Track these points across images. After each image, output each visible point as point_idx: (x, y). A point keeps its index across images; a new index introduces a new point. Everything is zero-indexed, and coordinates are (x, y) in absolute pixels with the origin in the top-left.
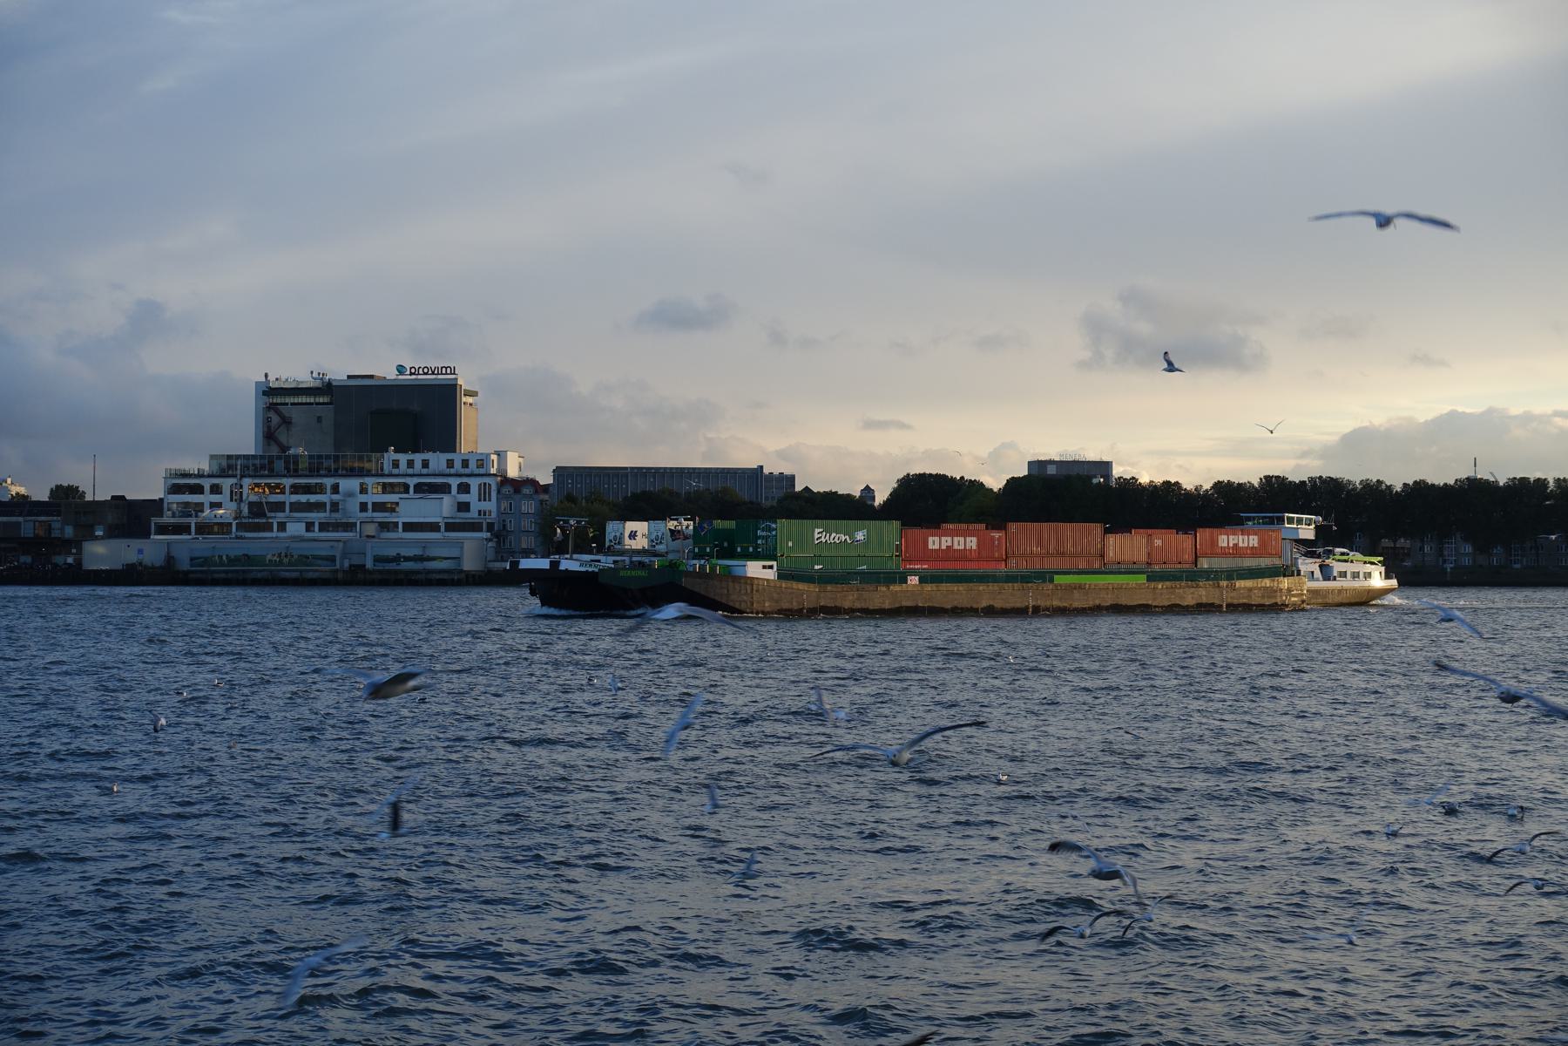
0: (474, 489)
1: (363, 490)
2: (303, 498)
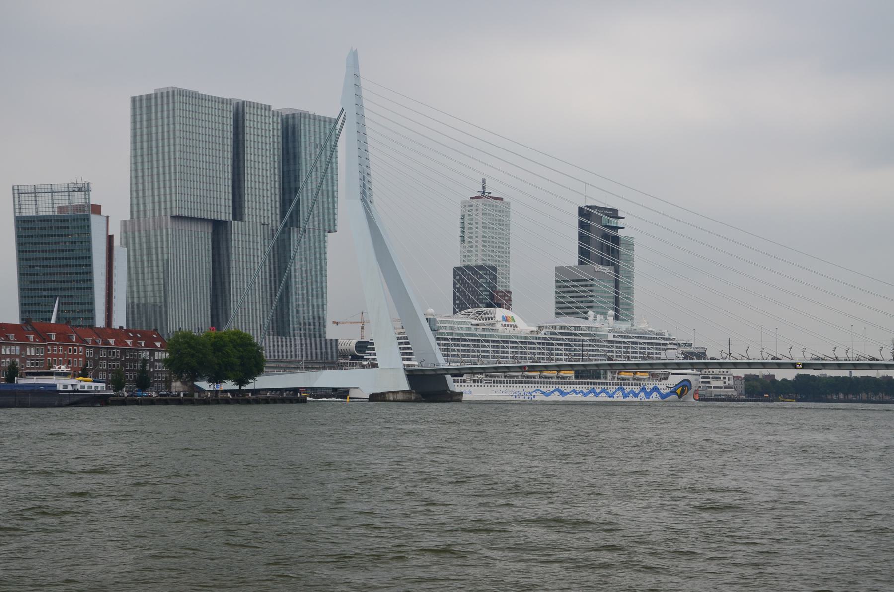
0: (727, 379)
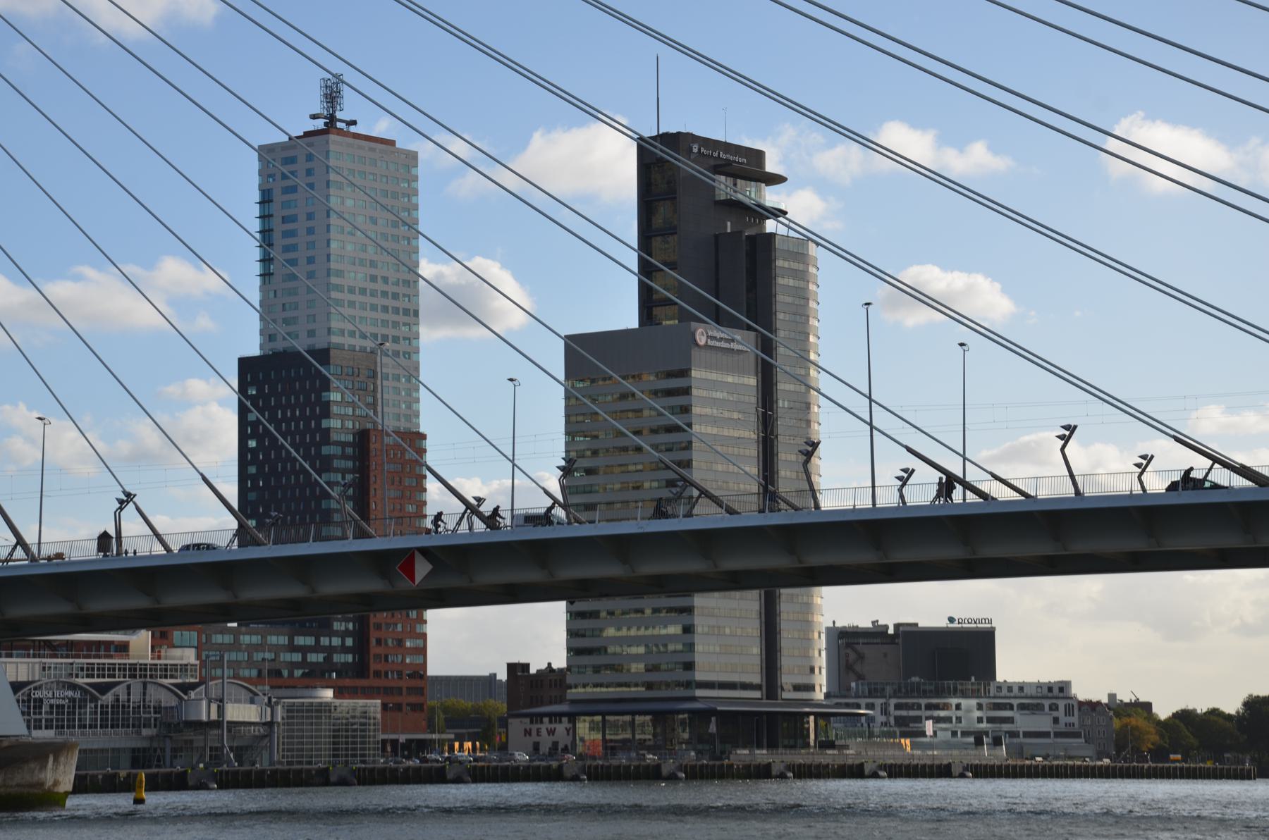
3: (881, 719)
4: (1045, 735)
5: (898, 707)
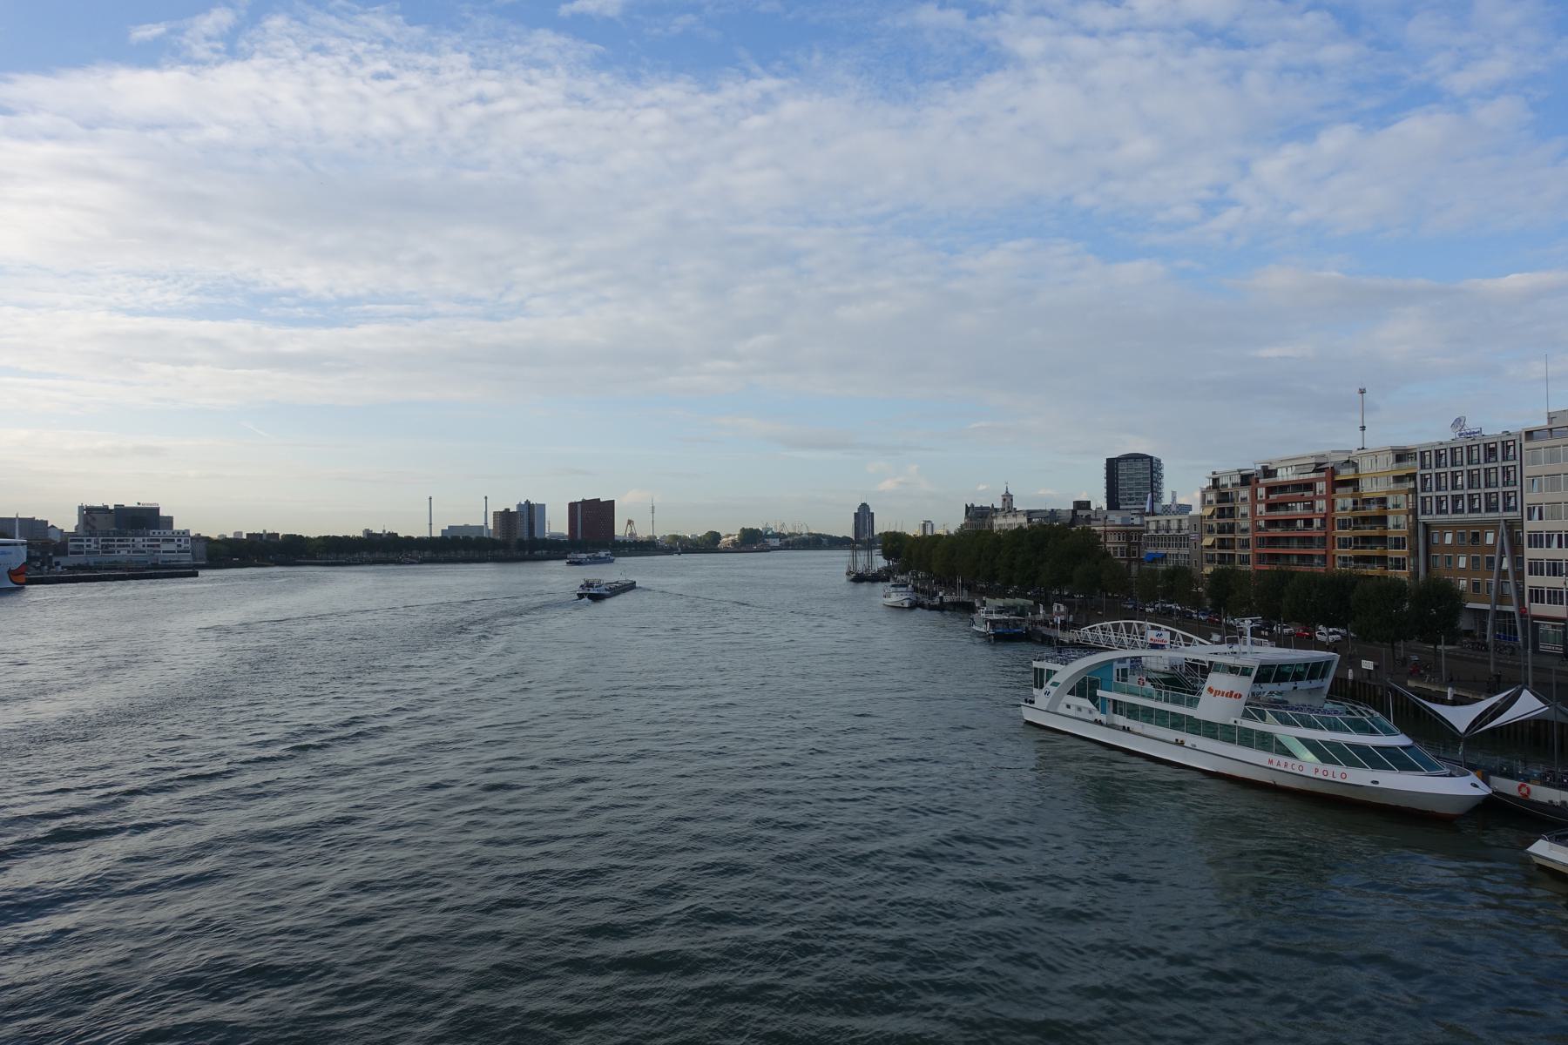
0: (183, 541)
1: (144, 541)
2: (122, 543)
3: (93, 546)
4: (174, 552)
5: (103, 541)
